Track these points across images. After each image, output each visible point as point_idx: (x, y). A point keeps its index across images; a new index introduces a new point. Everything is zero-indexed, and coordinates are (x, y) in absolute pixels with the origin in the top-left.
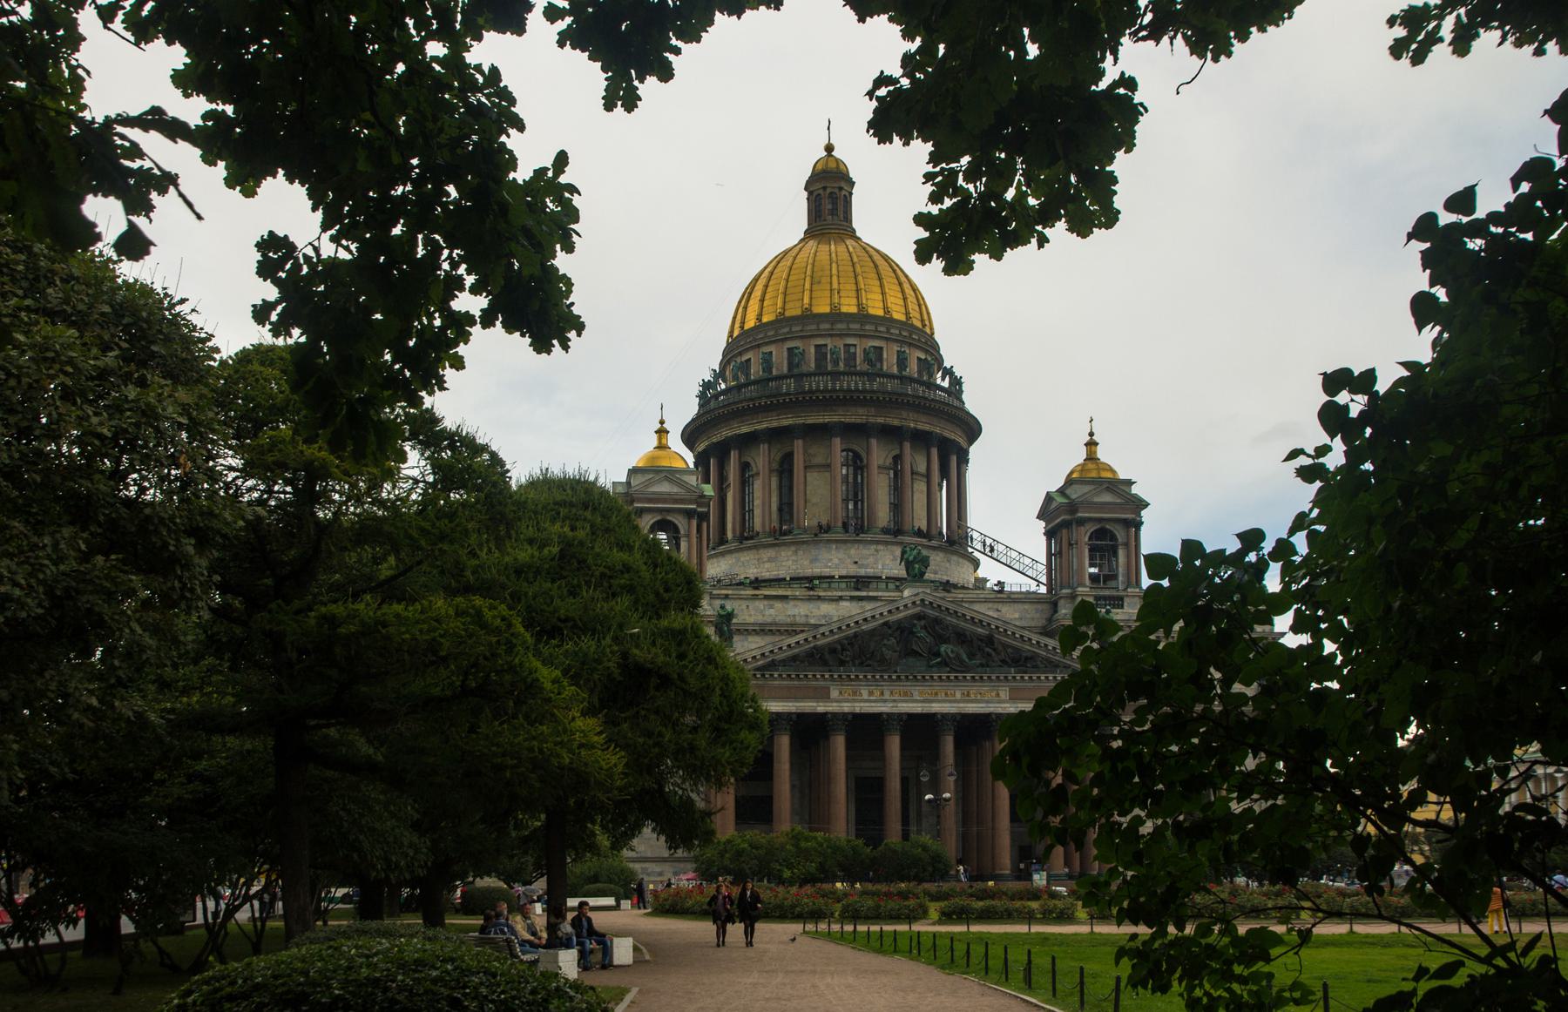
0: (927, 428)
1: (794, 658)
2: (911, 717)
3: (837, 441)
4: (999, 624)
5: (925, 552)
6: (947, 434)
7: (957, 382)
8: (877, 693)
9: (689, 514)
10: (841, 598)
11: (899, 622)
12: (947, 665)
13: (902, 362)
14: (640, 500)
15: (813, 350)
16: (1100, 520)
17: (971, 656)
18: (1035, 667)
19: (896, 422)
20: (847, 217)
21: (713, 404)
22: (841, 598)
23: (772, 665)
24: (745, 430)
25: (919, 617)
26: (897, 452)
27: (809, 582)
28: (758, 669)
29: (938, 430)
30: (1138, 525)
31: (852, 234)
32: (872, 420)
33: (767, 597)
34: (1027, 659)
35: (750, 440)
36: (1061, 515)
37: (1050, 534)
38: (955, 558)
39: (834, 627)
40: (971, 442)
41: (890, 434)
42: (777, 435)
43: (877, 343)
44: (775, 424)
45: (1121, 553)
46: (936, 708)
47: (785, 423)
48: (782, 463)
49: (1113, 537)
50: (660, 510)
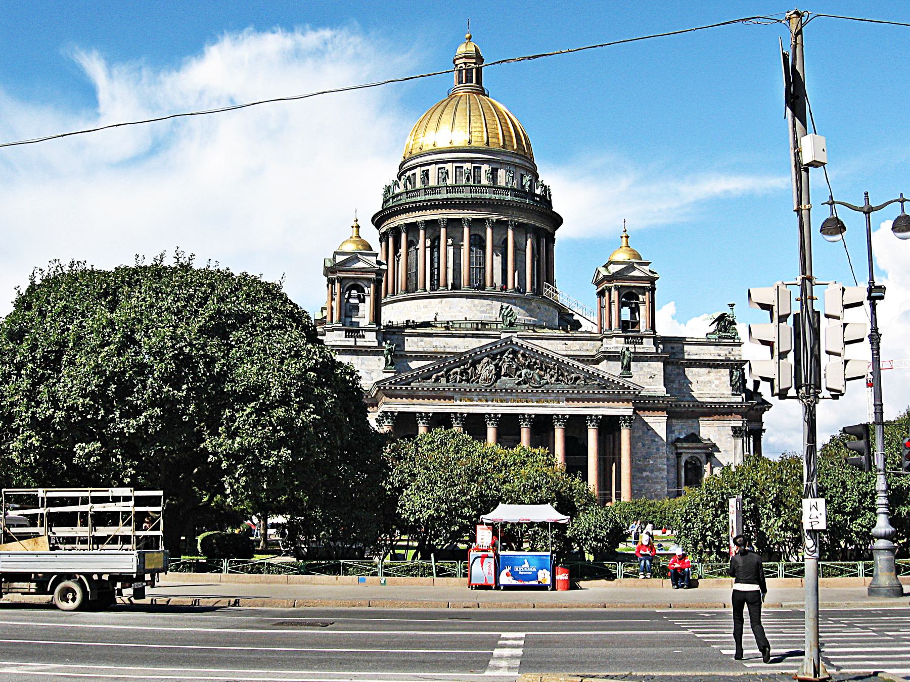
0: (525, 221)
3: (466, 230)
4: (559, 357)
7: (546, 189)
11: (497, 354)
12: (525, 383)
17: (541, 377)
20: (479, 81)
21: (390, 204)
22: (465, 336)
26: (505, 237)
30: (653, 290)
31: (482, 92)
32: (489, 216)
33: (419, 335)
34: (577, 379)
35: (412, 228)
37: (601, 294)
42: (432, 225)
45: (642, 308)
48: (432, 242)
50: (354, 279)
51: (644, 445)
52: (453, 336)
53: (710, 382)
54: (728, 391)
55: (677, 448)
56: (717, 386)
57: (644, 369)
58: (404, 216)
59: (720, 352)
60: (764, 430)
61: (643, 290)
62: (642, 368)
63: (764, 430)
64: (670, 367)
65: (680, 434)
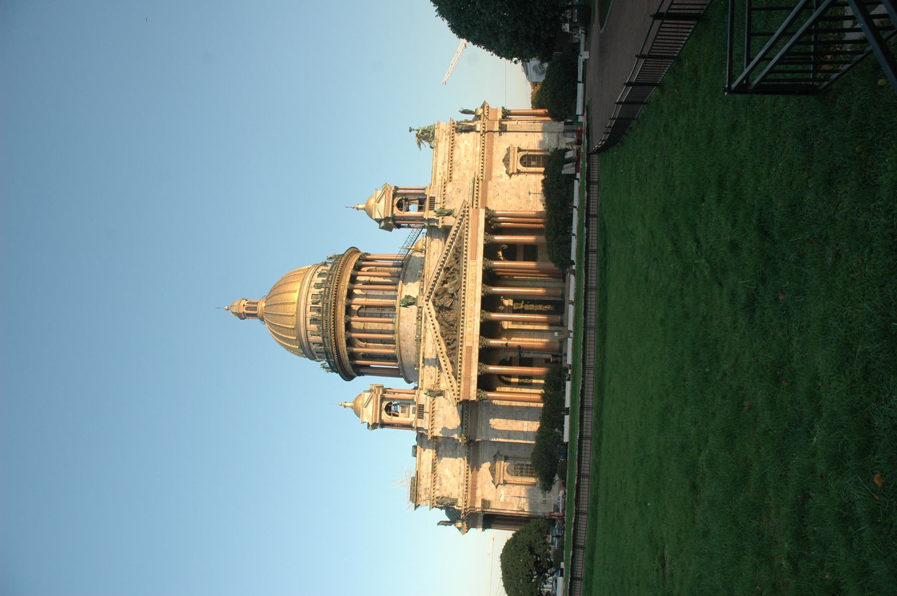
1: (452, 363)
2: (482, 308)
5: (403, 297)
6: (352, 267)
7: (331, 258)
8: (470, 324)
9: (383, 399)
13: (318, 286)
15: (312, 326)
19: (346, 292)
23: (453, 373)
24: (347, 358)
25: (434, 303)
27: (418, 340)
28: (456, 378)
29: (350, 271)
30: (397, 188)
32: (344, 303)
37: (399, 226)
38: (410, 265)
39: (437, 343)
40: (358, 252)
41: (350, 295)
46: (479, 295)
47: (344, 342)
49: (401, 200)
50: (381, 411)
53: (466, 147)
54: (472, 134)
58: (344, 362)
61: (395, 195)
64: (455, 177)
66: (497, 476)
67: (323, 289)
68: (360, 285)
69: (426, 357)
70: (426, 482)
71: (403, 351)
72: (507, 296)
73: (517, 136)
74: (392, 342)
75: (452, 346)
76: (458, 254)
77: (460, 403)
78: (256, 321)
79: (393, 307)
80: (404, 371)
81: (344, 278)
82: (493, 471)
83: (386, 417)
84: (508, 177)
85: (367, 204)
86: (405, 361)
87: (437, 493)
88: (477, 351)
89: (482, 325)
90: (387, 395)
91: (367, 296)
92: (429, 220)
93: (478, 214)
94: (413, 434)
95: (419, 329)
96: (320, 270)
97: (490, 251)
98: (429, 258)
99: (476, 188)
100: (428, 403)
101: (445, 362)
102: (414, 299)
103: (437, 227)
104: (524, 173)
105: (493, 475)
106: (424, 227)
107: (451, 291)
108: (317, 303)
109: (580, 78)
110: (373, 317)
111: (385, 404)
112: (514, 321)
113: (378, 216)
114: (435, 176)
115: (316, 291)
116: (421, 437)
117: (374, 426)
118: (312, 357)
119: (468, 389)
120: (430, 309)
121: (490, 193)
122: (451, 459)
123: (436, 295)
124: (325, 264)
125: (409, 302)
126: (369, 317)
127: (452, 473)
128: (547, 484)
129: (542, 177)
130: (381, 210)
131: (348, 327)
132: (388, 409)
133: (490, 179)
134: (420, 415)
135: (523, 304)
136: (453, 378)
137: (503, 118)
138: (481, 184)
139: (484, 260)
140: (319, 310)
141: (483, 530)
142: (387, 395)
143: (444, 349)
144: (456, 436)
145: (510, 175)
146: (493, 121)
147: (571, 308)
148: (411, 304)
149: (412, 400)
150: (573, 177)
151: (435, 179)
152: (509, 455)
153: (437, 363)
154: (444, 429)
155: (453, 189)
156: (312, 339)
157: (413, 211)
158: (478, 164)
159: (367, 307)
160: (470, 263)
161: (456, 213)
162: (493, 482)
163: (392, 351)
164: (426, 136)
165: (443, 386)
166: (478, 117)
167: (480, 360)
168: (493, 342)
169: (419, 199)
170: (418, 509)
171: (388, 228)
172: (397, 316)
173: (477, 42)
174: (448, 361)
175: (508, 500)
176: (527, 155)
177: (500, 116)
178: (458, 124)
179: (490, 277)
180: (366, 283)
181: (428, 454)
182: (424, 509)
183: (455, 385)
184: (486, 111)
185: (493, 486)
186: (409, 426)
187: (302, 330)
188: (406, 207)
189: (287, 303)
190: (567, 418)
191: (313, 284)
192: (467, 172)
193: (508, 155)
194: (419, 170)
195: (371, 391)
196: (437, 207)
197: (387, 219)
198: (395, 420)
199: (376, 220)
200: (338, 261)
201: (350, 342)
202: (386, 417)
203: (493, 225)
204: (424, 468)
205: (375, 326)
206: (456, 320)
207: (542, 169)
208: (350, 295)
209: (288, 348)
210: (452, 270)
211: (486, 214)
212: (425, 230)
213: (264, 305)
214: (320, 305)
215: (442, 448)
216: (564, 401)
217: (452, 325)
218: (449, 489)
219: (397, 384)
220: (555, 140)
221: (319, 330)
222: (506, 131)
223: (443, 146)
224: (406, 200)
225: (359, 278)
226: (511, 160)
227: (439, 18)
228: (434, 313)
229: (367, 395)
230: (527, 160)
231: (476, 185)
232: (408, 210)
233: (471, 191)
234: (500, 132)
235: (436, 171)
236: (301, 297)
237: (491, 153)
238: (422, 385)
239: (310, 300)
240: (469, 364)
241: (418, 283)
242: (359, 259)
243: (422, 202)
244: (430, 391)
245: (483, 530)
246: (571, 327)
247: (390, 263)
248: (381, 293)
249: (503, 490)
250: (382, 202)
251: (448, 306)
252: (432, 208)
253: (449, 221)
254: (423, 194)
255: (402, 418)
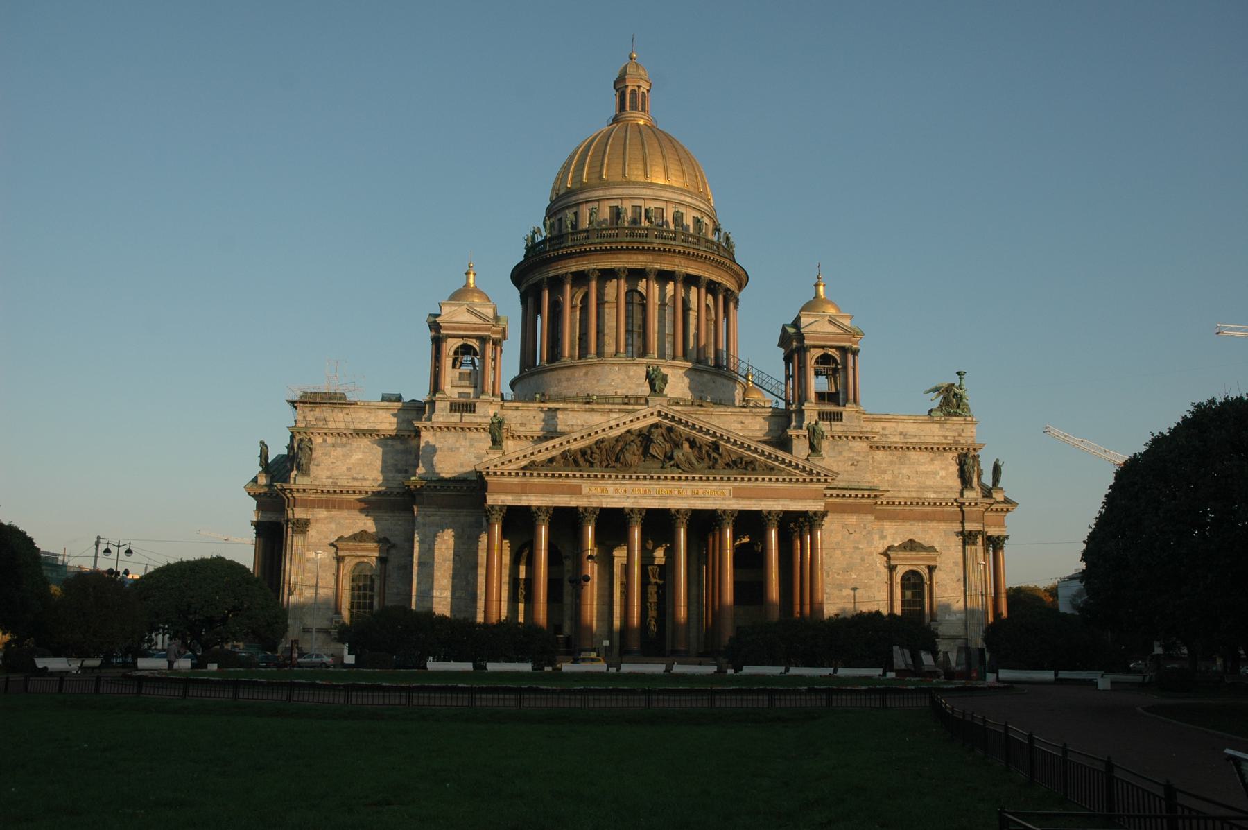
1: (551, 460)
5: (664, 371)
6: (713, 278)
7: (728, 239)
9: (483, 340)
10: (611, 411)
11: (640, 430)
13: (678, 218)
14: (446, 329)
15: (607, 210)
16: (823, 347)
17: (700, 459)
18: (754, 469)
19: (669, 268)
22: (611, 411)
23: (533, 464)
24: (552, 274)
25: (655, 426)
27: (588, 400)
28: (522, 469)
29: (706, 275)
30: (855, 353)
32: (649, 266)
36: (793, 344)
37: (788, 359)
38: (720, 380)
39: (584, 433)
40: (740, 288)
41: (664, 277)
43: (659, 204)
44: (574, 269)
46: (671, 504)
47: (581, 268)
49: (835, 361)
50: (462, 337)
51: (843, 554)
52: (593, 410)
53: (935, 473)
55: (889, 558)
56: (942, 478)
57: (845, 454)
59: (947, 434)
60: (1007, 537)
61: (843, 350)
62: (840, 453)
63: (1007, 537)
64: (880, 455)
65: (894, 540)
66: (351, 545)
67: (672, 227)
68: (681, 292)
69: (560, 415)
70: (338, 419)
71: (567, 372)
72: (671, 554)
73: (956, 563)
74: (584, 352)
75: (581, 461)
76: (743, 465)
77: (481, 477)
78: (612, 111)
79: (644, 352)
80: (532, 375)
81: (694, 265)
82: (361, 537)
83: (451, 346)
84: (881, 550)
85: (826, 301)
86: (550, 377)
87: (319, 440)
88: (573, 504)
89: (620, 511)
90: (489, 347)
91: (663, 305)
92: (801, 413)
93: (815, 499)
94: (423, 395)
95: (606, 399)
96: (706, 220)
97: (750, 522)
98: (733, 414)
99: (860, 494)
100: (479, 420)
101: (552, 448)
102: (662, 390)
103: (788, 426)
104: (891, 578)
105: (354, 538)
106: (788, 403)
107: (678, 454)
108: (647, 217)
109: (1063, 675)
110: (627, 317)
111: (474, 343)
112: (627, 569)
113: (805, 321)
114: (880, 420)
115: (668, 215)
116: (417, 410)
117: (435, 326)
118: (553, 211)
119: (506, 489)
120: (644, 418)
121: (852, 519)
122: (379, 463)
123: (670, 430)
124: (717, 229)
125: (655, 381)
126: (627, 310)
127: (355, 466)
128: (343, 634)
129: (885, 612)
130: (817, 327)
131: (608, 275)
132: (466, 349)
133: (878, 518)
134: (456, 407)
135: (659, 582)
136: (524, 463)
137: (989, 538)
138: (869, 503)
139: (733, 511)
140: (635, 221)
141: (253, 523)
142: (489, 347)
143: (575, 446)
144: (421, 470)
145: (885, 554)
146: (982, 520)
147: (659, 668)
148: (652, 386)
149: (483, 392)
150: (888, 665)
151: (874, 420)
152: (390, 566)
153: (550, 433)
154: (433, 450)
155: (858, 453)
156: (585, 211)
157: (817, 384)
158: (903, 495)
159: (644, 308)
160: (728, 487)
161: (815, 460)
162: (340, 539)
163: (567, 353)
164: (951, 401)
165: (509, 445)
166: (987, 493)
167: (557, 509)
168: (590, 532)
169: (837, 393)
170: (289, 406)
171: (785, 340)
172: (629, 361)
173: (1110, 500)
174: (554, 453)
175: (308, 565)
176: (922, 583)
177: (993, 531)
178: (975, 458)
179: (704, 523)
180: (685, 303)
181: (387, 422)
182: (288, 417)
183: (512, 467)
184: (999, 507)
185: (333, 538)
186: (436, 387)
187: (599, 193)
188: (822, 370)
189: (645, 164)
190: (468, 666)
191: (682, 209)
192: (888, 477)
193: (922, 548)
194: (889, 391)
195: (496, 318)
196: (824, 426)
197: (800, 337)
198: (447, 362)
199: (798, 318)
200: (723, 253)
201: (580, 279)
202: (451, 346)
203: (796, 526)
204: (363, 414)
205: (610, 322)
206: (626, 466)
207: (898, 610)
208: (664, 277)
209: (566, 168)
210: (713, 456)
211: (815, 513)
212: (782, 405)
213: (642, 123)
214: (645, 223)
215: (399, 446)
216: (496, 659)
217: (617, 460)
218: (327, 461)
219: (509, 363)
220: (952, 632)
221: (600, 223)
222: (964, 543)
223: (934, 433)
224: (835, 371)
225: (694, 290)
226: (913, 554)
227: (1148, 439)
228: (637, 426)
229: (489, 312)
230: (914, 582)
231: (866, 493)
232: (817, 374)
233: (855, 485)
234: (962, 533)
235: (889, 421)
236: (658, 187)
237: (925, 517)
238: (510, 409)
239: (652, 205)
240: (550, 490)
241: (688, 395)
242: (727, 290)
243: (832, 398)
244: (501, 423)
245: (253, 523)
246: (626, 668)
247: (722, 346)
248: (668, 330)
249: (326, 556)
250: (831, 329)
251: (651, 451)
252: (823, 416)
253: (801, 448)
254: (846, 400)
255: (450, 374)
